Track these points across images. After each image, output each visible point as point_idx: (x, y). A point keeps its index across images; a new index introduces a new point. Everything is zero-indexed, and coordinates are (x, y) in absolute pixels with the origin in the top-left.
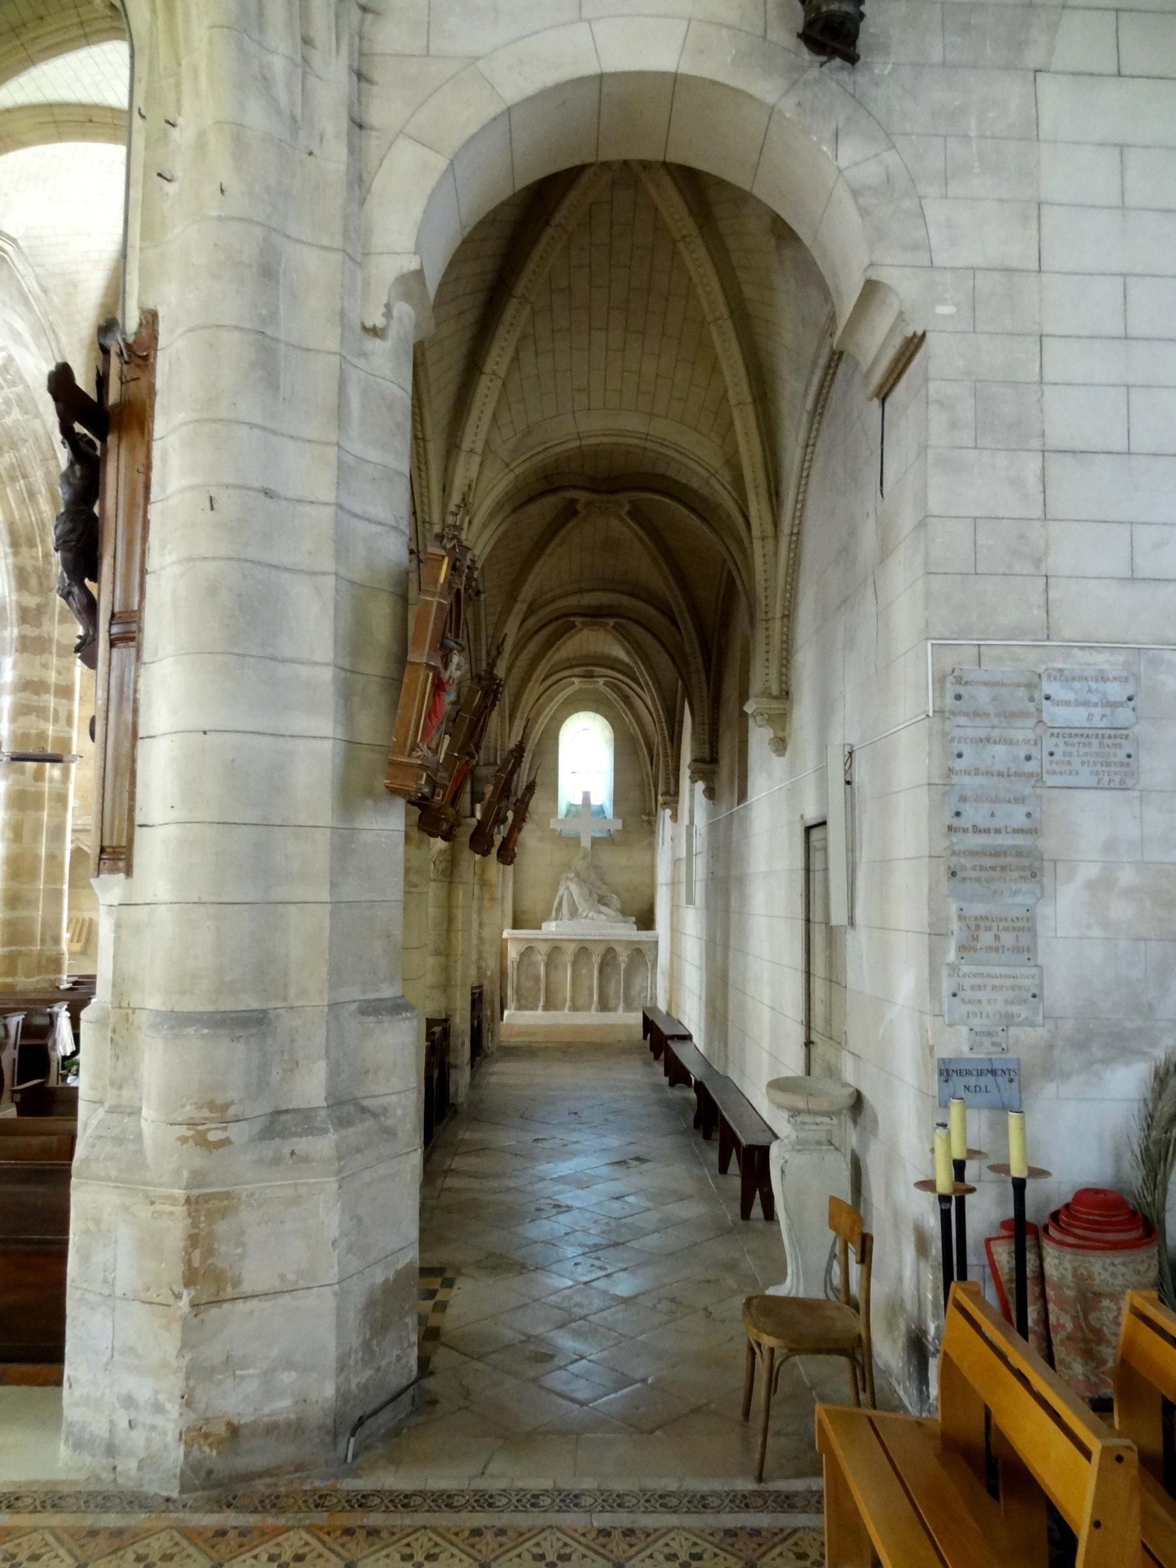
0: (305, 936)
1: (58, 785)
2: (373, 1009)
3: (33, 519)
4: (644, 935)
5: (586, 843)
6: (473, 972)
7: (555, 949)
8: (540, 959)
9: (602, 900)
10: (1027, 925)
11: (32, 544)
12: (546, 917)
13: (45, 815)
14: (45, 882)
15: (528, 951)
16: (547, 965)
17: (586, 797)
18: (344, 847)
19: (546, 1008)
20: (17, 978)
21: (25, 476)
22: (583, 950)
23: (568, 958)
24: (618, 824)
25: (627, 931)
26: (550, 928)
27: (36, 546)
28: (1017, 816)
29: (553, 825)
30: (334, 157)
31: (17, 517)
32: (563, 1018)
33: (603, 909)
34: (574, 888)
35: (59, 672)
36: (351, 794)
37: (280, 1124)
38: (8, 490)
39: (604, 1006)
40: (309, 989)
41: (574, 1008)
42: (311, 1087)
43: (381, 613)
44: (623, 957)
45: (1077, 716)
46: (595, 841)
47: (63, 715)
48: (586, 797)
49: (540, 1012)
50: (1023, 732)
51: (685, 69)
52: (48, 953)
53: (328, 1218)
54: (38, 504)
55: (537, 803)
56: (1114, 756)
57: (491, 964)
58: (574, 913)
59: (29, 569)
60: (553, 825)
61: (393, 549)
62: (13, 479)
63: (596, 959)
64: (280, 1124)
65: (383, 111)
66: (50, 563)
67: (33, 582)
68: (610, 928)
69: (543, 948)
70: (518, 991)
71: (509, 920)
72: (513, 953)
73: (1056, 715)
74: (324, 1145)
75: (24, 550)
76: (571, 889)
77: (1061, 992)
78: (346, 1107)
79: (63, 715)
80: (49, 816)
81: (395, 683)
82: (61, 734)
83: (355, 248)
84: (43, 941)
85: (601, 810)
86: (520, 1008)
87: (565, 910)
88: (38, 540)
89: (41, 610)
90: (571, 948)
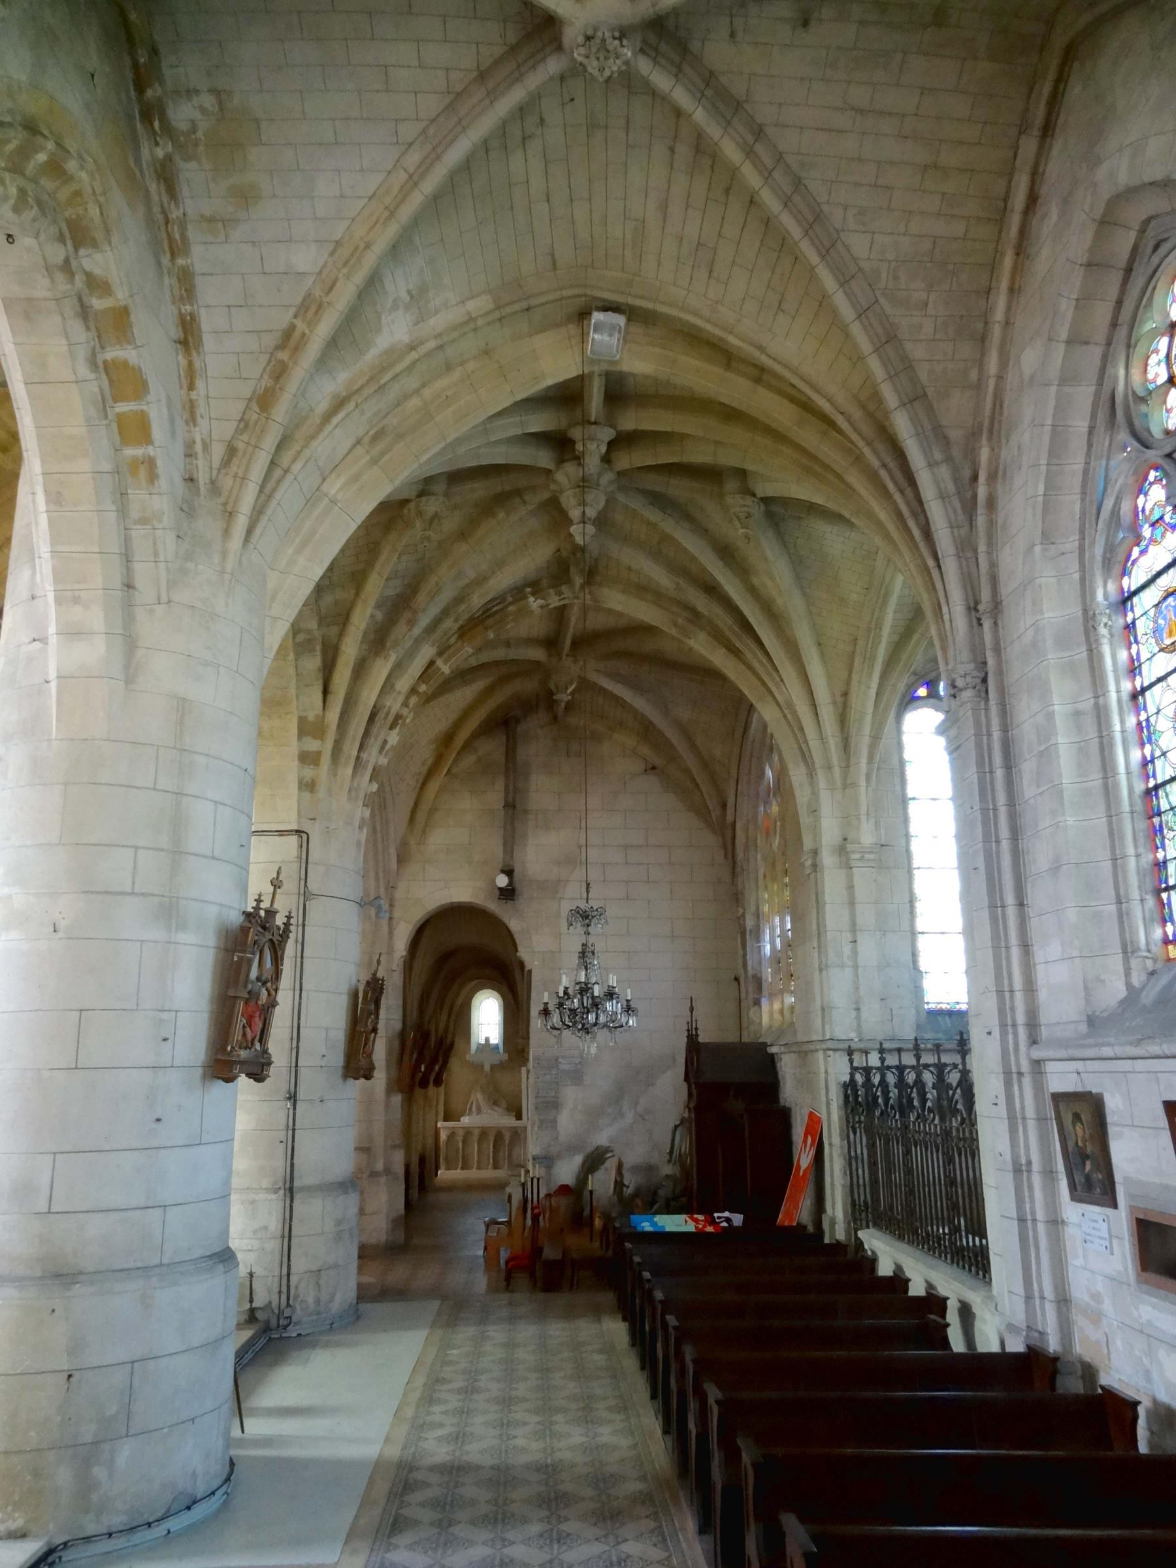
0: (379, 1126)
2: (394, 1147)
4: (518, 1123)
5: (487, 1068)
6: (420, 1146)
7: (468, 1132)
8: (460, 1139)
9: (495, 1103)
10: (555, 1121)
12: (463, 1114)
15: (452, 1135)
16: (464, 1142)
17: (487, 1039)
18: (387, 1105)
19: (462, 1168)
22: (484, 1133)
23: (475, 1138)
24: (506, 1057)
25: (509, 1121)
26: (466, 1120)
28: (553, 1094)
29: (468, 1058)
30: (385, 929)
32: (473, 1174)
33: (496, 1108)
34: (480, 1096)
36: (389, 1091)
37: (373, 1175)
39: (496, 1167)
40: (379, 1142)
41: (479, 1168)
42: (380, 1166)
43: (396, 1043)
44: (507, 1136)
45: (566, 1067)
46: (492, 1067)
48: (487, 1039)
49: (459, 1171)
50: (554, 1072)
51: (473, 900)
53: (383, 1197)
55: (459, 1044)
56: (577, 1076)
57: (430, 1141)
58: (479, 1111)
60: (468, 1058)
61: (399, 1026)
63: (492, 1139)
64: (373, 1175)
65: (397, 914)
68: (497, 1119)
69: (461, 1133)
70: (446, 1159)
71: (441, 1115)
72: (443, 1136)
73: (562, 1067)
74: (383, 1179)
76: (478, 1097)
77: (562, 1138)
78: (387, 1171)
81: (401, 1060)
83: (391, 950)
85: (496, 1047)
86: (448, 1169)
87: (474, 1109)
90: (476, 1132)
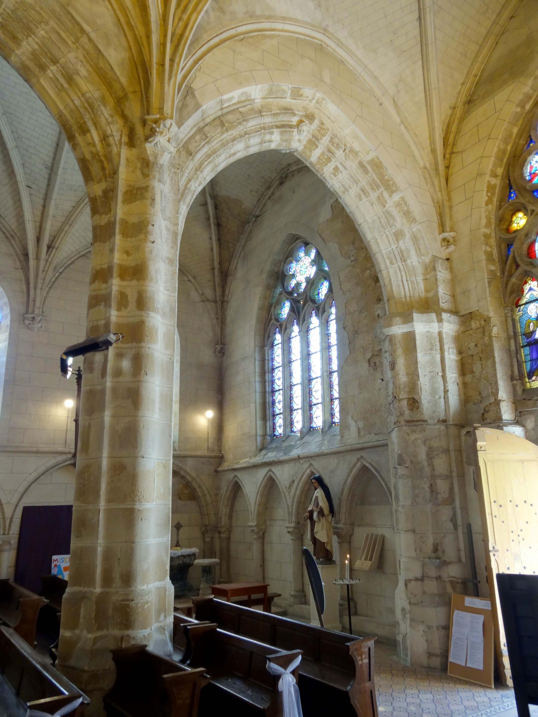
1: (127, 379)
3: (77, 102)
11: (85, 131)
13: (107, 416)
14: (109, 501)
20: (77, 632)
21: (55, 62)
27: (88, 131)
31: (61, 107)
35: (128, 253)
38: (42, 81)
47: (132, 298)
52: (114, 598)
54: (77, 85)
59: (88, 156)
62: (43, 68)
66: (109, 145)
67: (95, 169)
75: (79, 139)
79: (132, 298)
80: (113, 416)
82: (132, 319)
84: (107, 580)
88: (90, 124)
89: (109, 195)
